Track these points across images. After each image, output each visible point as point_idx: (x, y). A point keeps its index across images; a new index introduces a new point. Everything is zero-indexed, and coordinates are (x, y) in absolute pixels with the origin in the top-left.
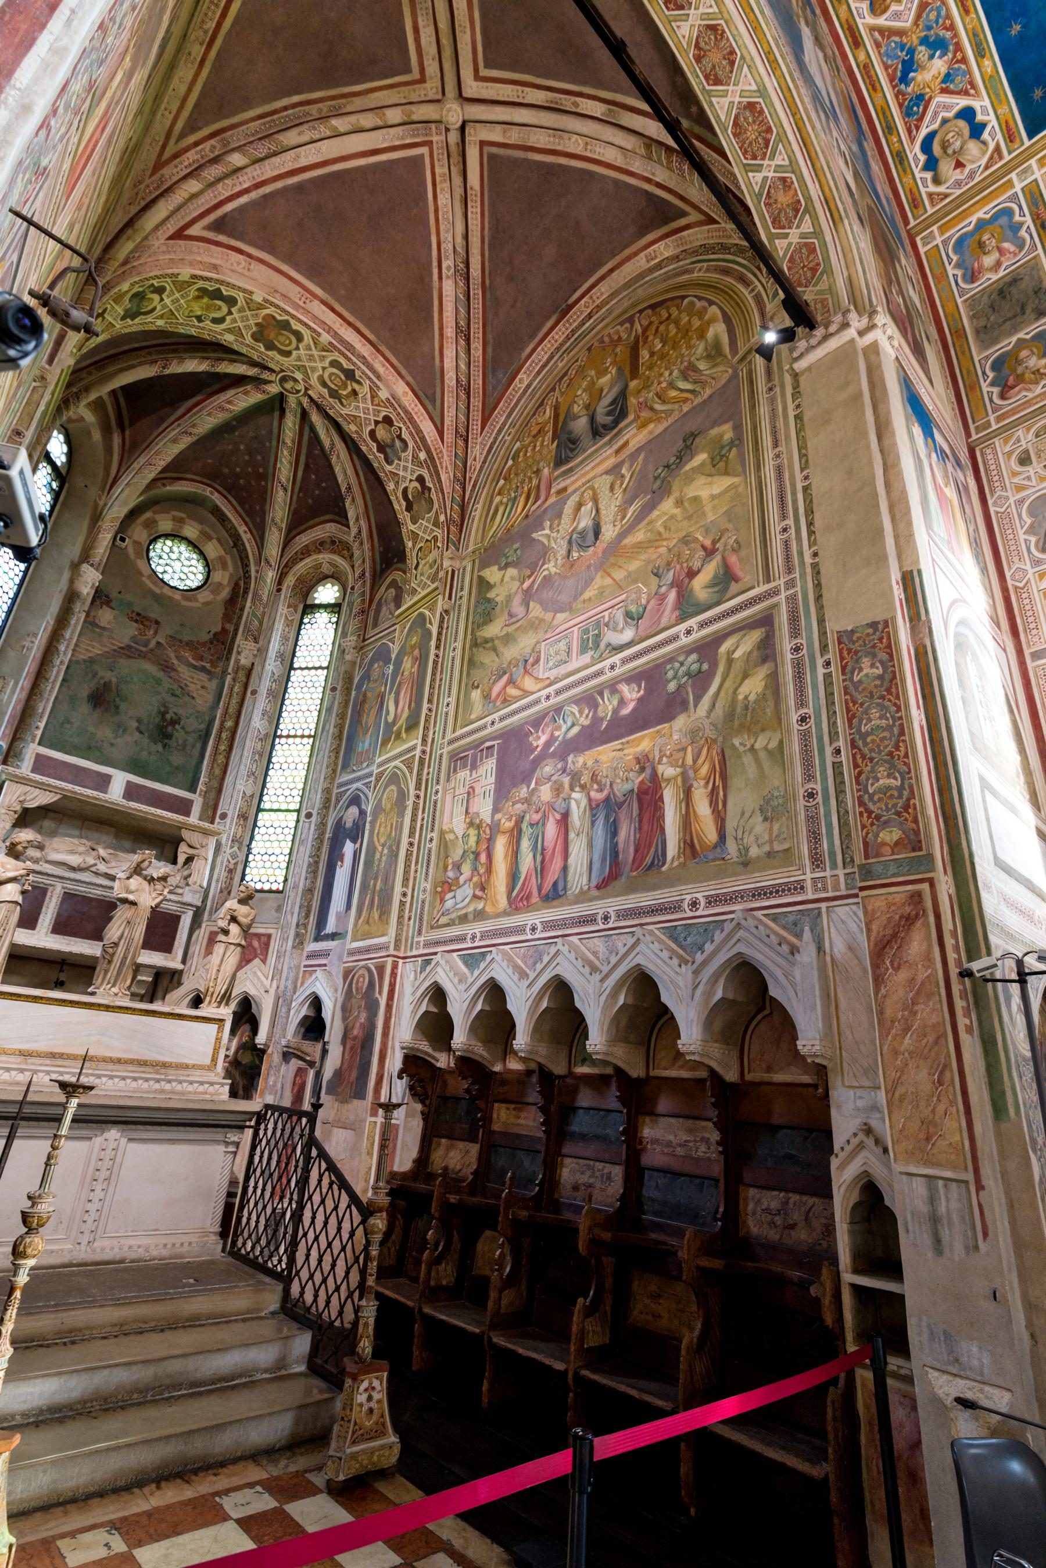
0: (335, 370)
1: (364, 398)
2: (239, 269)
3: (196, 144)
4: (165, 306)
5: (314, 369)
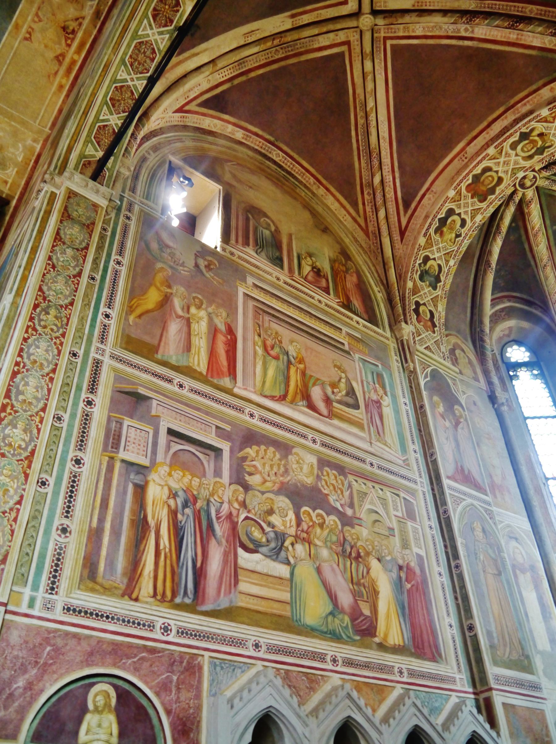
0: (519, 147)
1: (547, 128)
2: (433, 200)
3: (364, 204)
4: (440, 258)
5: (516, 163)
